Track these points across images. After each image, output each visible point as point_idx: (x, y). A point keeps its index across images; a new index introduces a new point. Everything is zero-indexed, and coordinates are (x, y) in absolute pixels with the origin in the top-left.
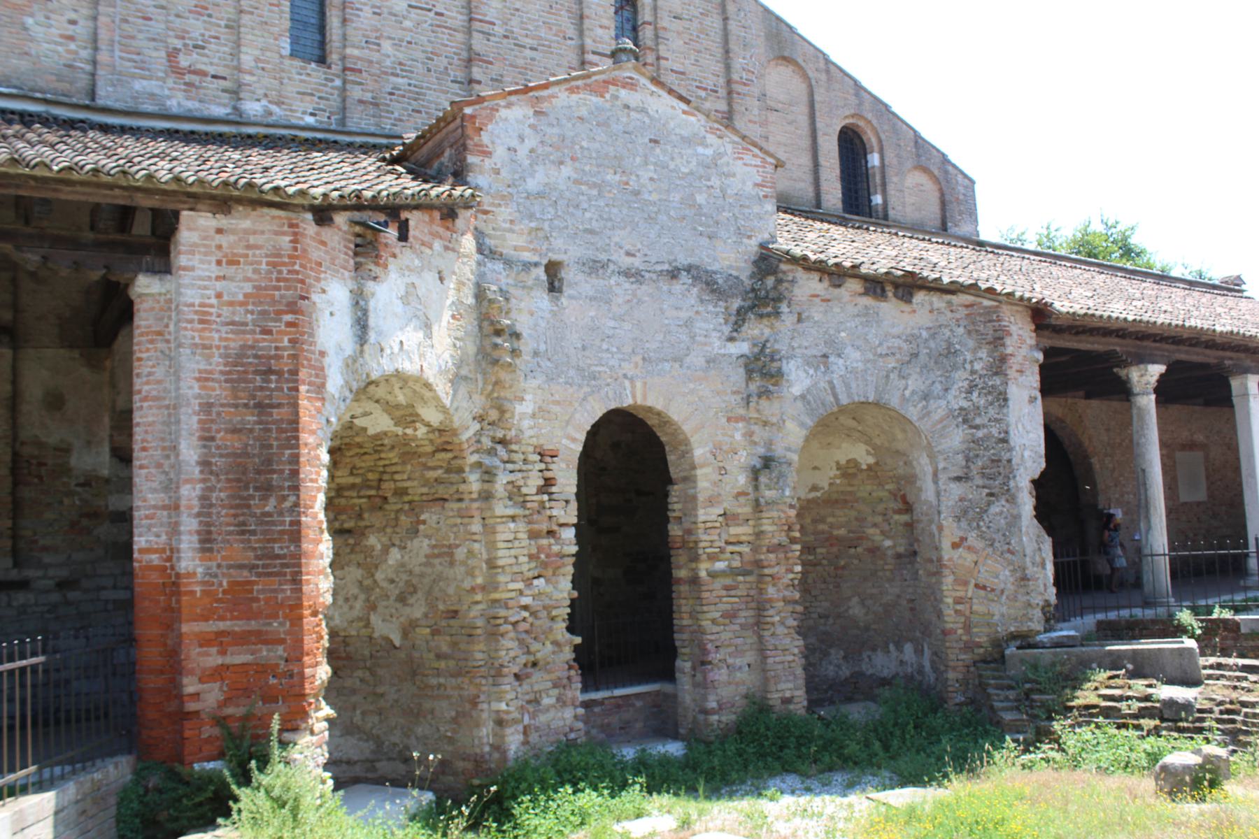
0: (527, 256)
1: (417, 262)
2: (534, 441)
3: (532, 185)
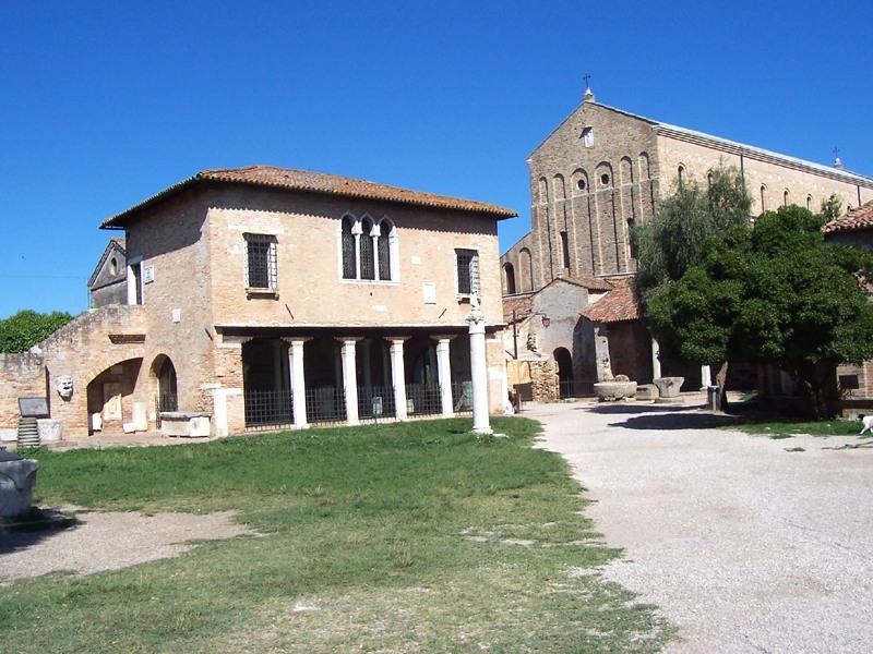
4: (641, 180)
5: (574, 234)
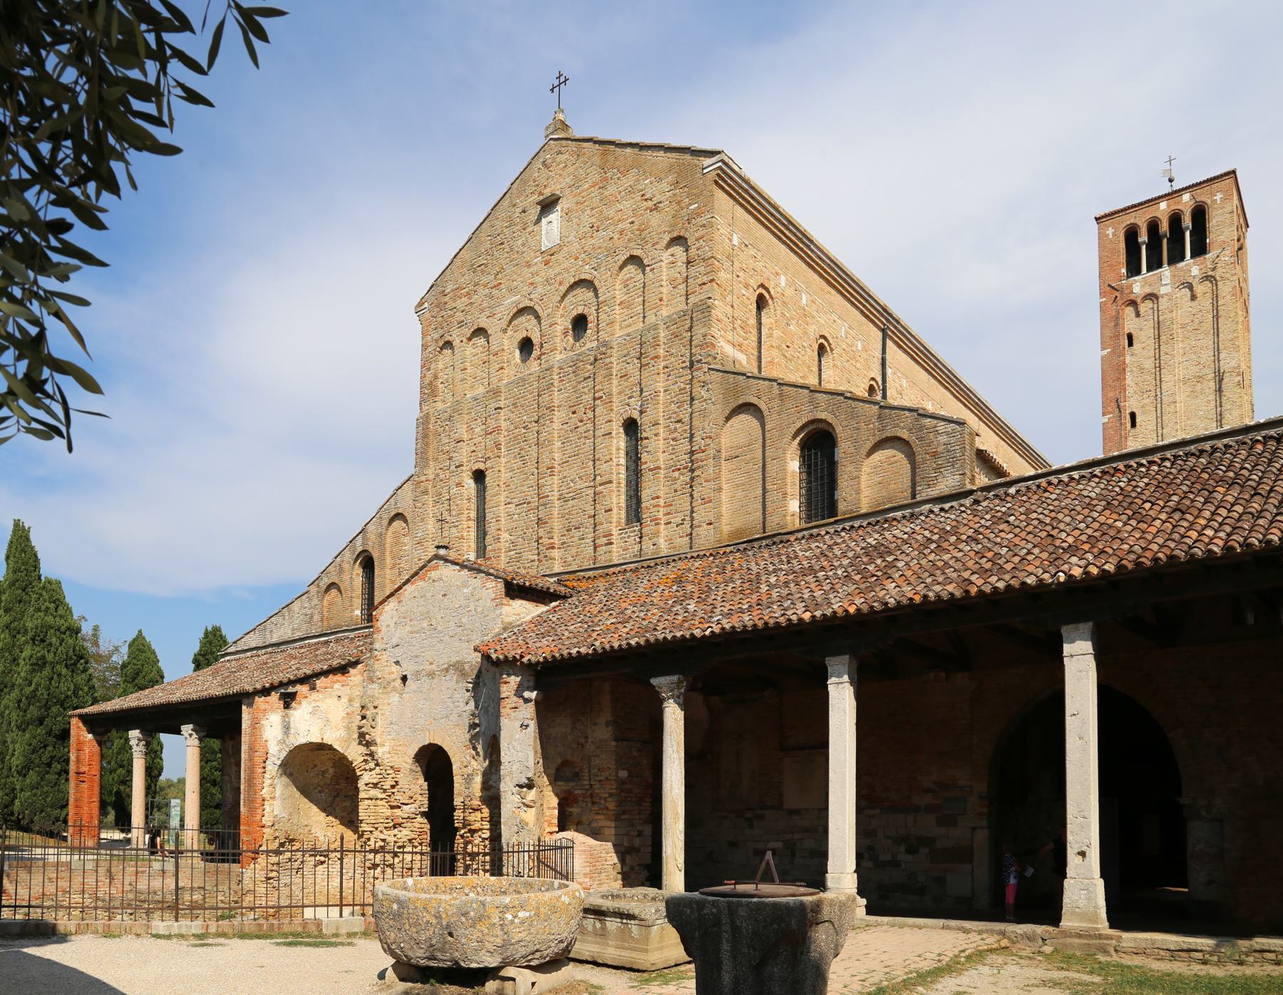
0: (393, 676)
1: (321, 697)
2: (390, 764)
3: (395, 641)
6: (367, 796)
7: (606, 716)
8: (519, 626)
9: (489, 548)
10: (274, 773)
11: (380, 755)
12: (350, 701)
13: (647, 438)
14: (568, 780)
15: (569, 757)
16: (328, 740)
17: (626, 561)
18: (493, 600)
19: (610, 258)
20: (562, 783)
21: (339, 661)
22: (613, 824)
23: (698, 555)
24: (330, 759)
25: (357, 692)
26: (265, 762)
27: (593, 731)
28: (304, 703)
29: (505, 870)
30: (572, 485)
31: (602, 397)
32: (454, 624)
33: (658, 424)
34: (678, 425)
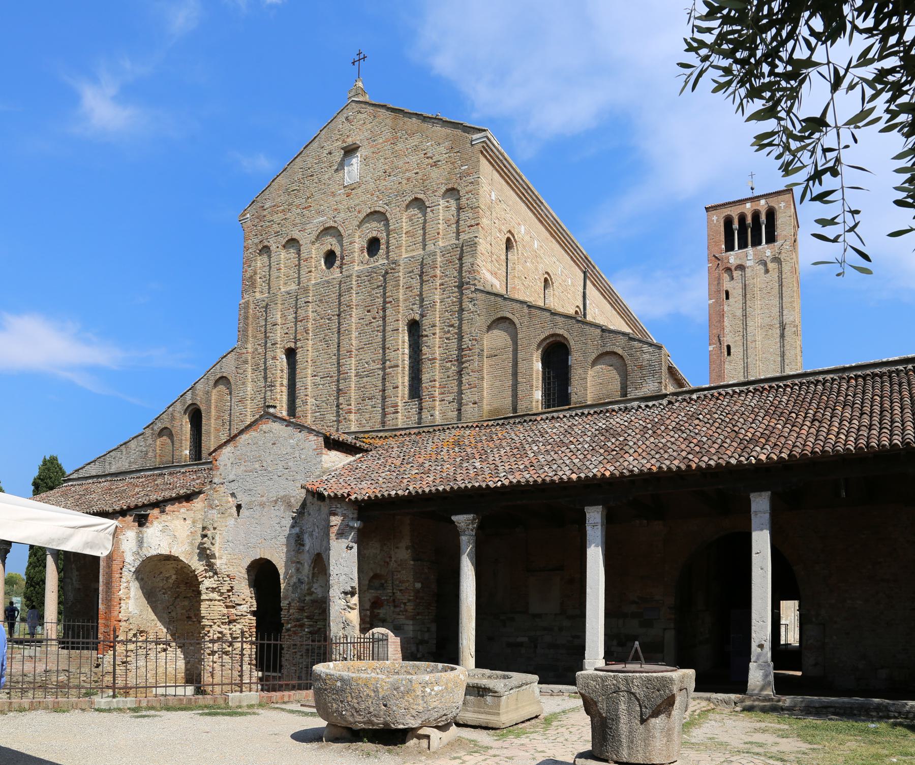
2: (226, 573)
3: (231, 477)
4: (441, 243)
5: (308, 354)
6: (207, 598)
7: (406, 542)
8: (334, 471)
9: (298, 409)
10: (129, 578)
11: (218, 565)
12: (194, 522)
13: (427, 336)
14: (376, 589)
15: (378, 572)
16: (175, 552)
17: (409, 426)
18: (315, 450)
19: (399, 198)
20: (373, 591)
21: (185, 490)
22: (411, 622)
23: (467, 426)
24: (173, 568)
25: (199, 516)
26: (121, 569)
27: (396, 553)
28: (155, 523)
29: (334, 656)
30: (366, 366)
31: (392, 302)
32: (281, 467)
33: (435, 326)
34: (451, 329)
